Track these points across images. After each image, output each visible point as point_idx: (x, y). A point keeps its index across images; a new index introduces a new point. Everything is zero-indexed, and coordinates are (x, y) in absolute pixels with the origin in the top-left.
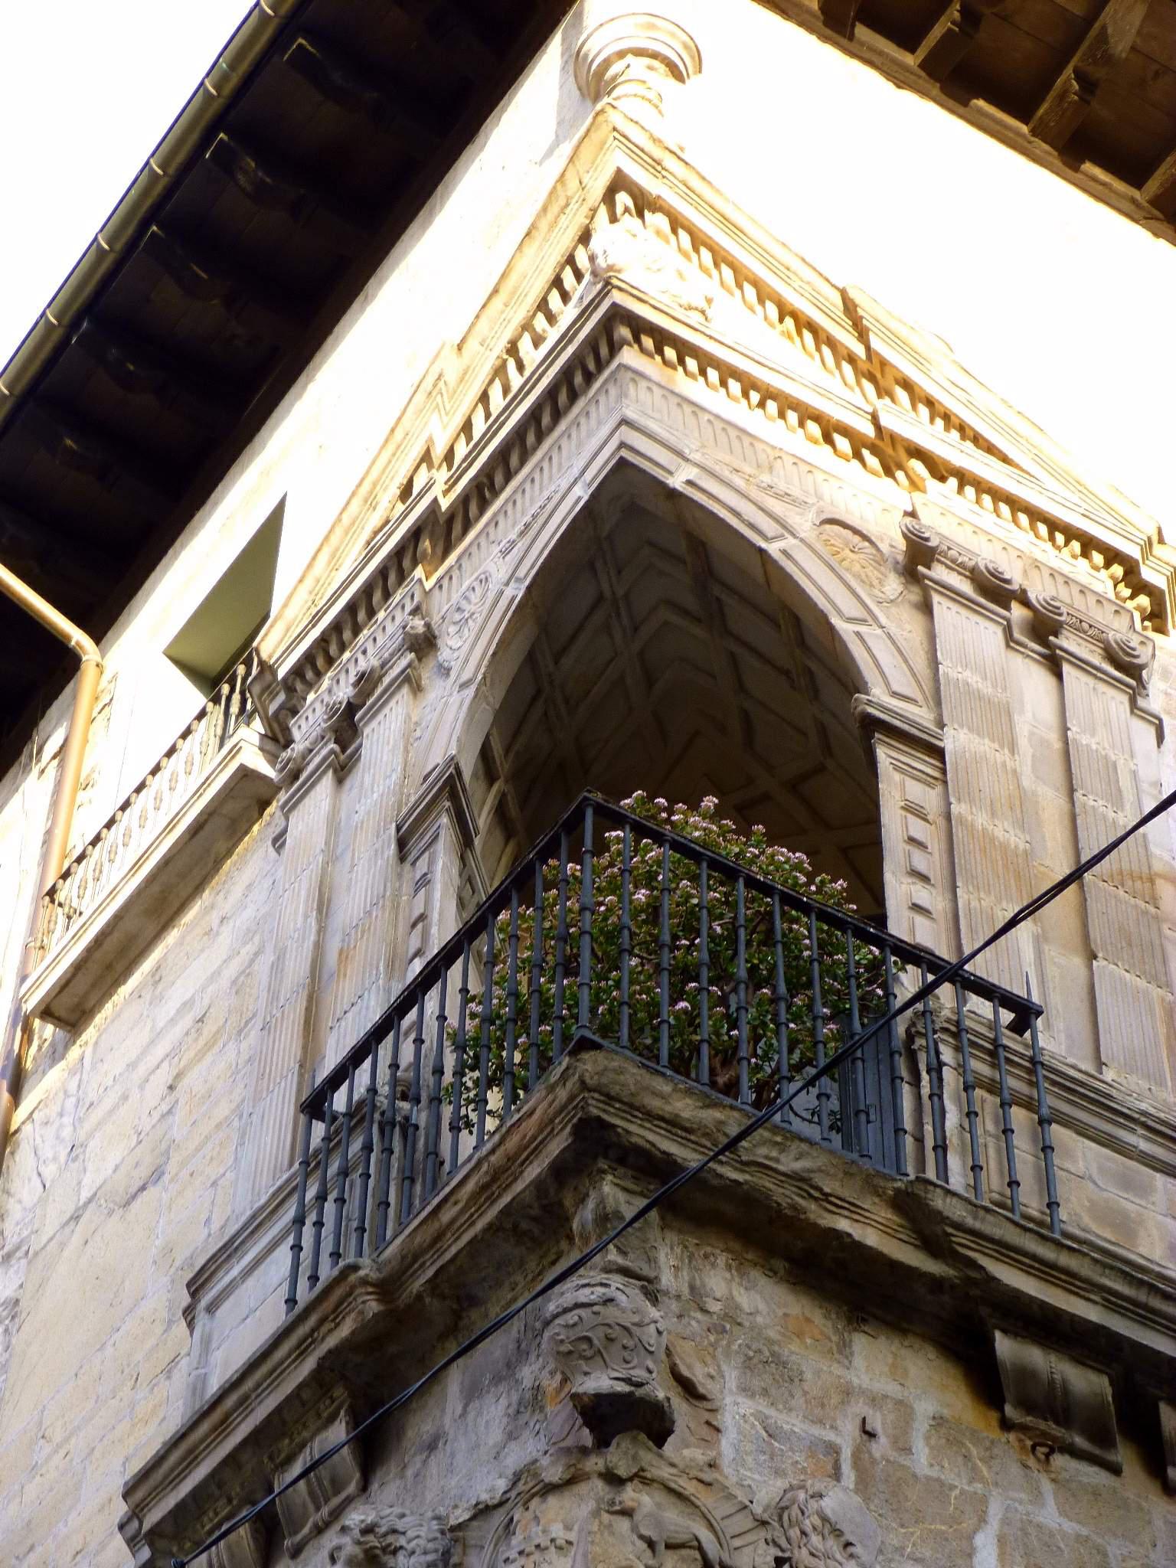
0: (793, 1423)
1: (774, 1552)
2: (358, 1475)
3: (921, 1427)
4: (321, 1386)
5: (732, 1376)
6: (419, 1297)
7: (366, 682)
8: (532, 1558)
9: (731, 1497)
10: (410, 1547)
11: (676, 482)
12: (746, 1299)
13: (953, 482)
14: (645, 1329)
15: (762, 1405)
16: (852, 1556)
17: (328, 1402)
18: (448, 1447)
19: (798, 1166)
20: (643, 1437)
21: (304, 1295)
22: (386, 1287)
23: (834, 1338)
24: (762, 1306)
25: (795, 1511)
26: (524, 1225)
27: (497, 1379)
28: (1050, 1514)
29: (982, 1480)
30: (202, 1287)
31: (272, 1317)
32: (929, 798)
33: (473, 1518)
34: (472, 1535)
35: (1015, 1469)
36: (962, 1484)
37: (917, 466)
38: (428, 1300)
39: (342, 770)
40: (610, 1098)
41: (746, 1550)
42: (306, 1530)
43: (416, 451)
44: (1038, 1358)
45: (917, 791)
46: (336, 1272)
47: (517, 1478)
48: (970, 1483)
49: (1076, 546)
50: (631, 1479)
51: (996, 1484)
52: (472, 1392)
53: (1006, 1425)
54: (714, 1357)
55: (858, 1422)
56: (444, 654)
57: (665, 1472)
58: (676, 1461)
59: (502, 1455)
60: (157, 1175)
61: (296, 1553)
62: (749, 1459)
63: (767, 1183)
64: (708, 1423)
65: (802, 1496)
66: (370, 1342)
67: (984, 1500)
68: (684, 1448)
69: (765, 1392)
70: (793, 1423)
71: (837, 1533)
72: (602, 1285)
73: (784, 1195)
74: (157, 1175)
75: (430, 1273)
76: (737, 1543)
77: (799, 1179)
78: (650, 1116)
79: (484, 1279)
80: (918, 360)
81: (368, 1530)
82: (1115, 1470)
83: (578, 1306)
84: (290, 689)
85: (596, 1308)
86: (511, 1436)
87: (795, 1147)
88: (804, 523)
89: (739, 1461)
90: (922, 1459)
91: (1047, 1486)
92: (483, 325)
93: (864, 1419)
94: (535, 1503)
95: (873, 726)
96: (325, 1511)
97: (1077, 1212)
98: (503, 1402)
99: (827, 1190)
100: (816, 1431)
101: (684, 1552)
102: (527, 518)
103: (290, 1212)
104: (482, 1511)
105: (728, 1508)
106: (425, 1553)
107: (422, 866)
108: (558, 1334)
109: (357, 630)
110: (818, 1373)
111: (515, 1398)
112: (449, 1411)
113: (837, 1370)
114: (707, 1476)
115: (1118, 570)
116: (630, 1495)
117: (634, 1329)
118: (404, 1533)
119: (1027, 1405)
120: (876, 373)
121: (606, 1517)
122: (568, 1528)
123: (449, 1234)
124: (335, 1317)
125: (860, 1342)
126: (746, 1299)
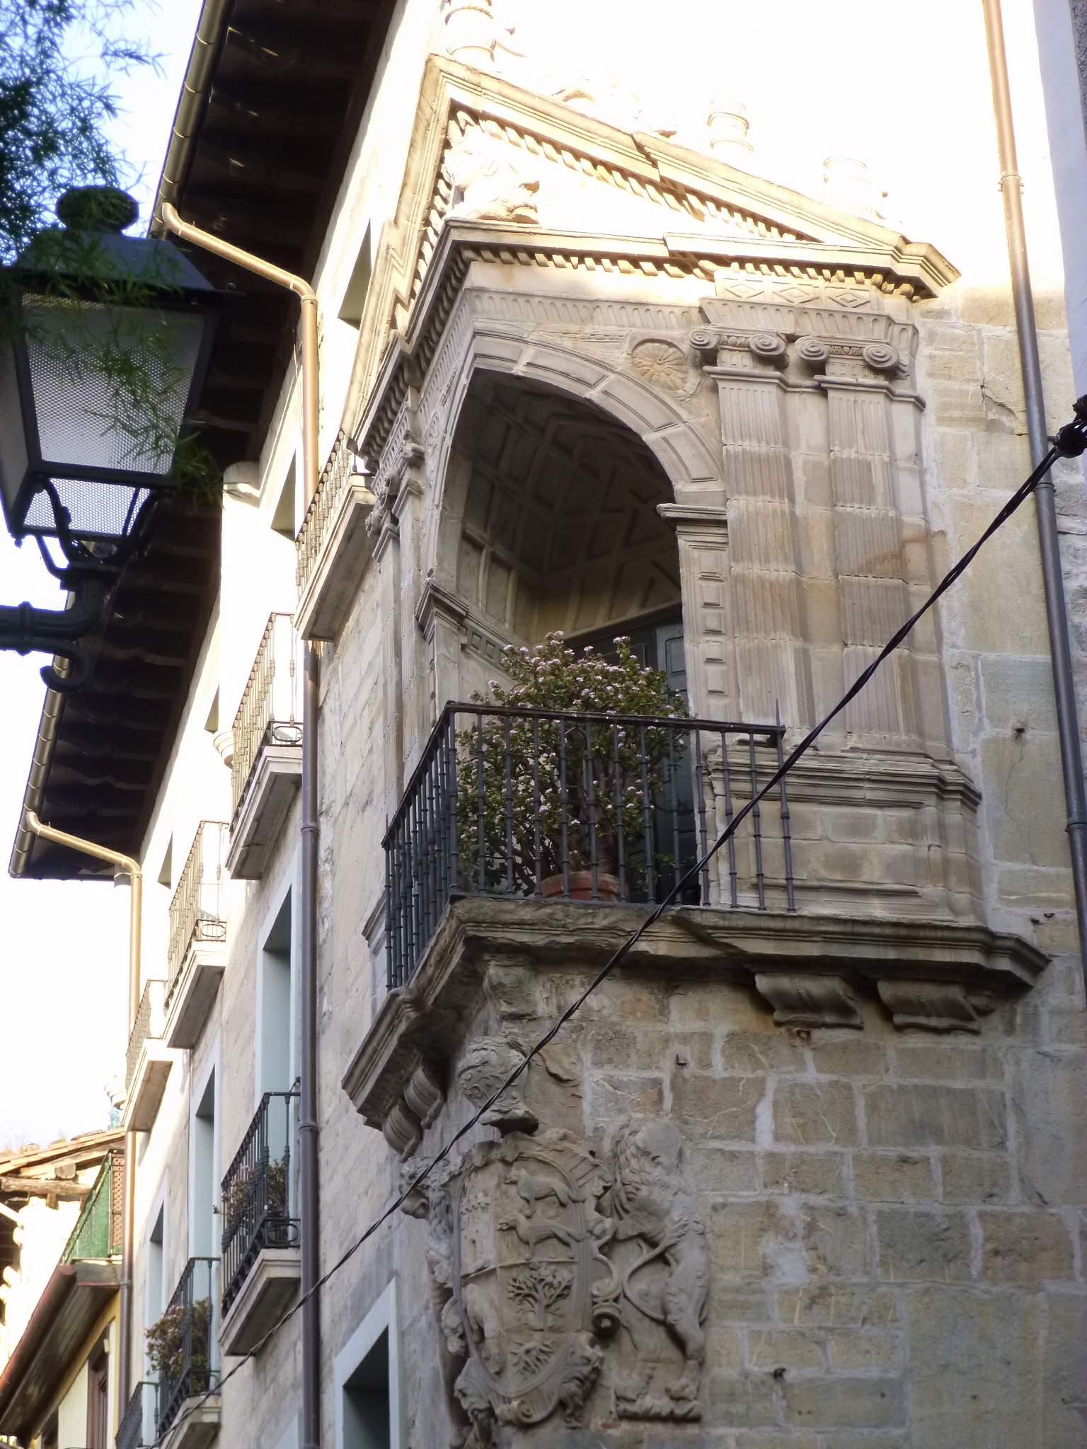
0: (630, 1074)
3: (718, 1045)
5: (587, 1057)
13: (735, 265)
15: (609, 1070)
19: (605, 923)
20: (519, 1133)
22: (417, 1003)
23: (657, 1006)
28: (812, 1075)
35: (785, 1051)
37: (706, 264)
40: (478, 923)
43: (389, 299)
44: (785, 983)
48: (754, 1071)
49: (840, 273)
54: (575, 1048)
55: (674, 1059)
62: (602, 1109)
63: (590, 937)
67: (762, 1082)
69: (610, 1061)
76: (581, 1182)
77: (610, 929)
78: (506, 924)
80: (699, 171)
82: (859, 1028)
87: (601, 913)
88: (619, 357)
89: (595, 1113)
90: (719, 1068)
91: (808, 1055)
92: (404, 208)
102: (448, 382)
105: (574, 1162)
110: (646, 1034)
113: (660, 1027)
115: (878, 278)
116: (514, 1173)
121: (504, 1186)
122: (486, 1195)
125: (675, 1002)
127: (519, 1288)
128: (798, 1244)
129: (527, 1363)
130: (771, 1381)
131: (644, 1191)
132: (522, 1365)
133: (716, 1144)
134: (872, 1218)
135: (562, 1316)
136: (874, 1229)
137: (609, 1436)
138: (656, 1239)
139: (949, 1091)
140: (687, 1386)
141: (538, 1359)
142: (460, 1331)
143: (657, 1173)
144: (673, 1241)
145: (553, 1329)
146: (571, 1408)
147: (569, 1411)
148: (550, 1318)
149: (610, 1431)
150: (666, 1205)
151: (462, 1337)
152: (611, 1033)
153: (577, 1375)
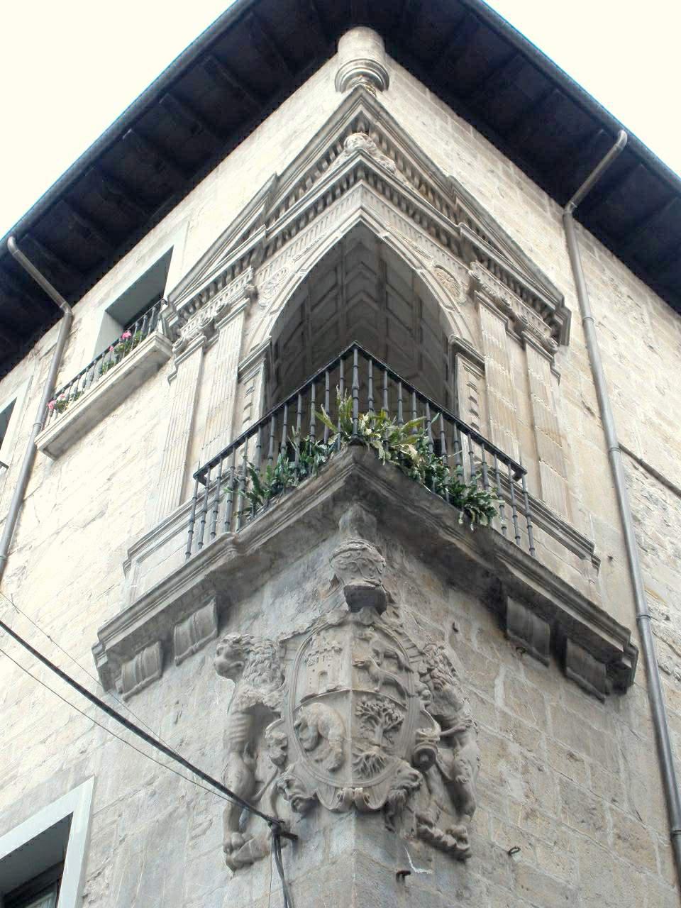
1: (427, 666)
2: (216, 629)
5: (403, 595)
6: (257, 551)
7: (224, 310)
9: (409, 640)
10: (256, 651)
11: (382, 235)
12: (407, 566)
16: (454, 675)
19: (438, 511)
24: (414, 570)
26: (314, 522)
27: (292, 589)
28: (522, 677)
29: (498, 658)
30: (137, 552)
31: (181, 561)
32: (478, 384)
33: (292, 637)
34: (291, 646)
38: (261, 553)
39: (206, 348)
42: (187, 652)
45: (473, 379)
47: (314, 622)
50: (369, 626)
51: (503, 661)
52: (278, 594)
53: (506, 637)
56: (261, 300)
57: (383, 626)
58: (388, 622)
60: (102, 514)
61: (179, 663)
64: (394, 613)
65: (435, 648)
66: (229, 571)
68: (387, 617)
69: (416, 605)
70: (425, 619)
71: (449, 664)
72: (360, 543)
73: (429, 523)
74: (102, 514)
75: (264, 541)
76: (411, 660)
77: (437, 517)
79: (288, 546)
81: (238, 642)
82: (546, 664)
83: (350, 549)
84: (181, 316)
91: (521, 664)
93: (454, 624)
95: (458, 349)
96: (197, 644)
97: (539, 556)
98: (296, 598)
99: (448, 524)
100: (435, 625)
101: (392, 660)
102: (308, 246)
103: (188, 517)
104: (296, 635)
106: (263, 653)
107: (249, 385)
109: (217, 291)
111: (302, 596)
112: (265, 601)
114: (401, 630)
118: (253, 645)
119: (516, 633)
120: (457, 215)
124: (211, 560)
126: (407, 566)
127: (366, 710)
128: (519, 776)
129: (365, 765)
130: (506, 856)
131: (448, 686)
132: (362, 765)
134: (557, 781)
135: (392, 743)
136: (558, 788)
137: (411, 845)
138: (451, 723)
139: (590, 728)
142: (285, 743)
143: (454, 679)
144: (464, 728)
145: (384, 749)
146: (391, 812)
147: (391, 813)
148: (385, 740)
149: (411, 843)
151: (284, 748)
153: (406, 785)
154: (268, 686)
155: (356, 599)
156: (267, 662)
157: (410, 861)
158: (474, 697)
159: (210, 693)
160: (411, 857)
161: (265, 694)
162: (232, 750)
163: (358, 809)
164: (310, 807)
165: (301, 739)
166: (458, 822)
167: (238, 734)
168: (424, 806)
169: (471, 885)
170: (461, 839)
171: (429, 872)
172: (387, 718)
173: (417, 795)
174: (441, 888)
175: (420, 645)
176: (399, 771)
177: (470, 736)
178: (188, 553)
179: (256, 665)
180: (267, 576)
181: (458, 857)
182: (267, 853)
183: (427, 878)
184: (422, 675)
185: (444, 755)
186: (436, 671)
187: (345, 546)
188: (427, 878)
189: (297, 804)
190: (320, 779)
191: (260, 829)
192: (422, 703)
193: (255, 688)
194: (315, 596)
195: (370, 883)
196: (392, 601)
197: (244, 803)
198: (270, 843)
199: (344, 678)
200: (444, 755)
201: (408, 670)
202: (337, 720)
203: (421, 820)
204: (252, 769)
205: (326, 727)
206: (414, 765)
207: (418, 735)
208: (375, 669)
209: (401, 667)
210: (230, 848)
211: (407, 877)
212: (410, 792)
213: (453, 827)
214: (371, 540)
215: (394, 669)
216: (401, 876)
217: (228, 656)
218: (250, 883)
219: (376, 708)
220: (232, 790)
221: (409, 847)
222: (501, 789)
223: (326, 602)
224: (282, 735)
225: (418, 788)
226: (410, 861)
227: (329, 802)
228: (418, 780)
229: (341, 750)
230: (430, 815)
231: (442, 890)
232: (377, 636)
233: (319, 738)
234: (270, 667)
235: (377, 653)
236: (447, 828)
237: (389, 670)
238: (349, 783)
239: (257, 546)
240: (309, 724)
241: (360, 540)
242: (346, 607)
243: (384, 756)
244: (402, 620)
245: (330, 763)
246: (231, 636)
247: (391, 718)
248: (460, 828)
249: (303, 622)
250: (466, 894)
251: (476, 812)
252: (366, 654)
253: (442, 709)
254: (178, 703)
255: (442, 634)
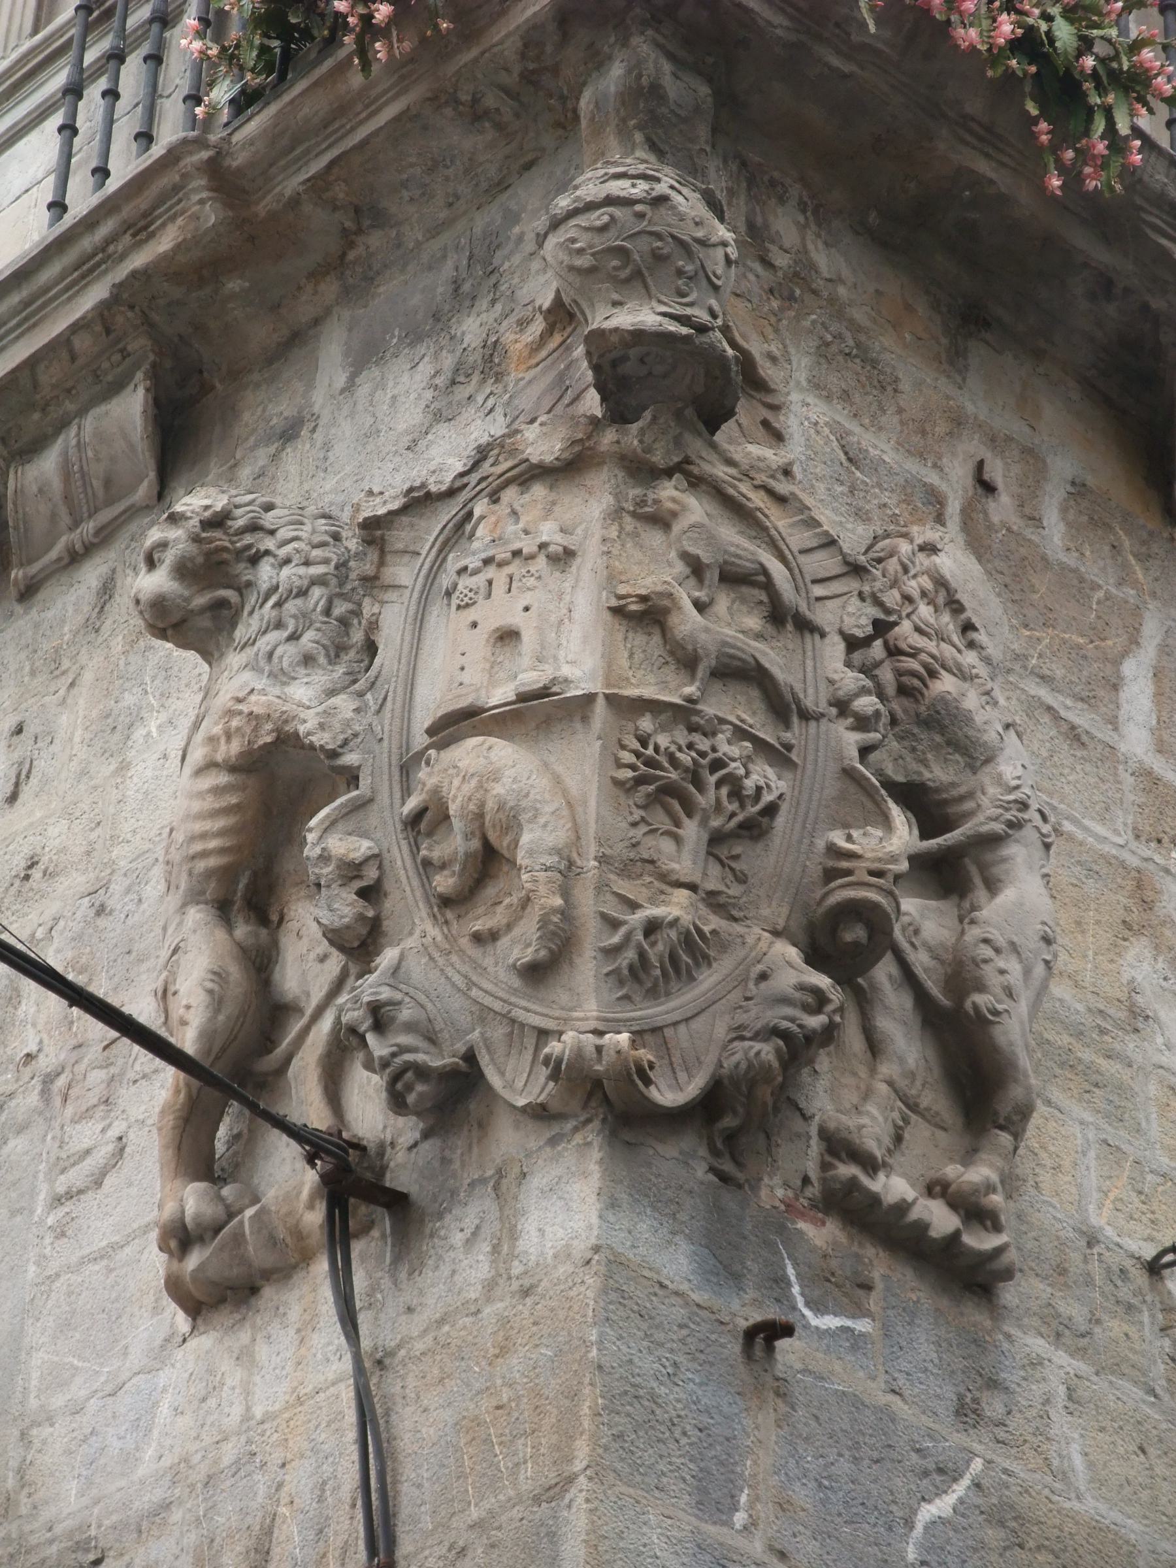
0: (881, 447)
1: (874, 612)
2: (152, 475)
4: (108, 331)
5: (801, 365)
6: (294, 202)
8: (508, 570)
9: (813, 523)
10: (283, 552)
12: (823, 259)
14: (711, 251)
15: (841, 415)
16: (971, 645)
17: (117, 357)
18: (319, 436)
21: (82, 199)
23: (944, 341)
24: (846, 272)
25: (893, 565)
26: (490, 101)
27: (414, 337)
29: (1135, 584)
33: (404, 510)
34: (399, 538)
36: (1108, 584)
38: (307, 208)
41: (829, 603)
42: (53, 554)
46: (95, 200)
47: (482, 453)
48: (1120, 584)
50: (669, 473)
51: (1153, 594)
52: (367, 355)
57: (721, 471)
58: (737, 457)
59: (422, 444)
62: (821, 487)
64: (765, 424)
65: (905, 547)
66: (200, 269)
67: (1137, 612)
68: (741, 446)
69: (846, 396)
71: (956, 607)
72: (644, 177)
75: (317, 166)
76: (818, 591)
79: (404, 185)
81: (217, 521)
83: (610, 201)
85: (639, 208)
86: (439, 417)
93: (980, 465)
94: (510, 495)
96: (89, 527)
98: (426, 368)
99: (969, 109)
100: (912, 466)
101: (745, 590)
103: (58, 79)
104: (420, 501)
105: (806, 538)
106: (307, 563)
108: (573, 240)
111: (448, 361)
112: (322, 380)
114: (783, 487)
116: (668, 492)
117: (696, 247)
118: (272, 532)
121: (629, 523)
123: (359, 107)
124: (141, 229)
126: (823, 259)
127: (650, 763)
129: (642, 955)
130: (1140, 1278)
131: (946, 684)
132: (630, 955)
133: (1043, 693)
135: (741, 879)
137: (800, 1232)
138: (952, 810)
140: (994, 1191)
141: (674, 958)
142: (371, 874)
143: (970, 658)
144: (998, 827)
145: (714, 901)
146: (735, 1119)
147: (729, 1122)
148: (715, 870)
149: (801, 1225)
150: (991, 736)
151: (371, 894)
152: (851, 343)
153: (785, 1024)
154: (321, 678)
155: (629, 377)
156: (317, 592)
157: (796, 1290)
158: (1046, 719)
159: (129, 699)
160: (799, 1275)
161: (309, 702)
162: (194, 897)
163: (611, 1105)
164: (451, 1097)
165: (427, 863)
166: (969, 1156)
167: (213, 844)
168: (850, 1097)
169: (1010, 1377)
170: (975, 1212)
171: (862, 1326)
172: (724, 791)
173: (824, 1061)
174: (902, 1381)
175: (854, 538)
176: (763, 977)
177: (1019, 855)
178: (58, 206)
179: (279, 605)
180: (330, 288)
181: (967, 1276)
182: (306, 1258)
183: (854, 1348)
184: (853, 644)
185: (922, 918)
186: (905, 627)
187: (590, 187)
188: (854, 1348)
189: (409, 1088)
190: (488, 1001)
191: (287, 1178)
192: (852, 740)
193: (273, 682)
194: (491, 362)
195: (647, 1364)
196: (756, 384)
197: (229, 1080)
198: (315, 1218)
199: (576, 649)
200: (922, 918)
201: (806, 626)
202: (551, 794)
203: (838, 1146)
204: (261, 963)
205: (512, 823)
206: (815, 957)
207: (834, 851)
208: (687, 621)
209: (780, 616)
210: (180, 1238)
211: (782, 1344)
212: (798, 1049)
213: (952, 1171)
214: (691, 170)
215: (754, 622)
216: (759, 1340)
217: (182, 571)
218: (245, 1357)
219: (685, 758)
220: (188, 1041)
221: (793, 1240)
222: (1130, 1045)
223: (528, 384)
224: (361, 848)
225: (828, 1035)
226: (796, 1290)
227: (516, 1081)
228: (829, 1008)
229: (558, 901)
230: (871, 1127)
231: (907, 1393)
232: (696, 509)
233: (489, 860)
234: (327, 612)
235: (696, 569)
236: (933, 1174)
237: (733, 625)
238: (586, 1017)
239: (292, 184)
240: (453, 809)
241: (640, 159)
242: (592, 403)
243: (713, 923)
244: (794, 451)
245: (523, 944)
246: (195, 502)
247: (736, 793)
248: (980, 1173)
249: (445, 458)
250: (994, 1406)
251: (1035, 1120)
252: (655, 571)
253: (924, 762)
254: (19, 730)
255: (936, 502)
